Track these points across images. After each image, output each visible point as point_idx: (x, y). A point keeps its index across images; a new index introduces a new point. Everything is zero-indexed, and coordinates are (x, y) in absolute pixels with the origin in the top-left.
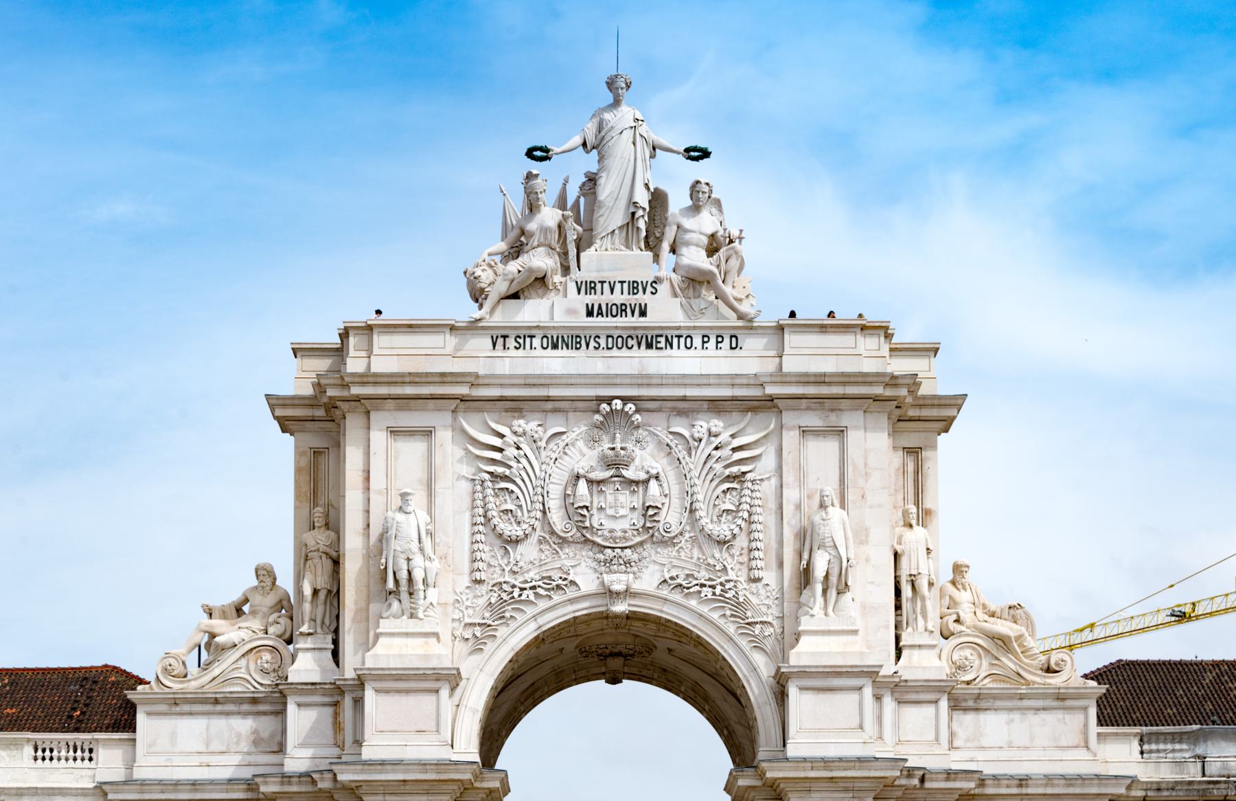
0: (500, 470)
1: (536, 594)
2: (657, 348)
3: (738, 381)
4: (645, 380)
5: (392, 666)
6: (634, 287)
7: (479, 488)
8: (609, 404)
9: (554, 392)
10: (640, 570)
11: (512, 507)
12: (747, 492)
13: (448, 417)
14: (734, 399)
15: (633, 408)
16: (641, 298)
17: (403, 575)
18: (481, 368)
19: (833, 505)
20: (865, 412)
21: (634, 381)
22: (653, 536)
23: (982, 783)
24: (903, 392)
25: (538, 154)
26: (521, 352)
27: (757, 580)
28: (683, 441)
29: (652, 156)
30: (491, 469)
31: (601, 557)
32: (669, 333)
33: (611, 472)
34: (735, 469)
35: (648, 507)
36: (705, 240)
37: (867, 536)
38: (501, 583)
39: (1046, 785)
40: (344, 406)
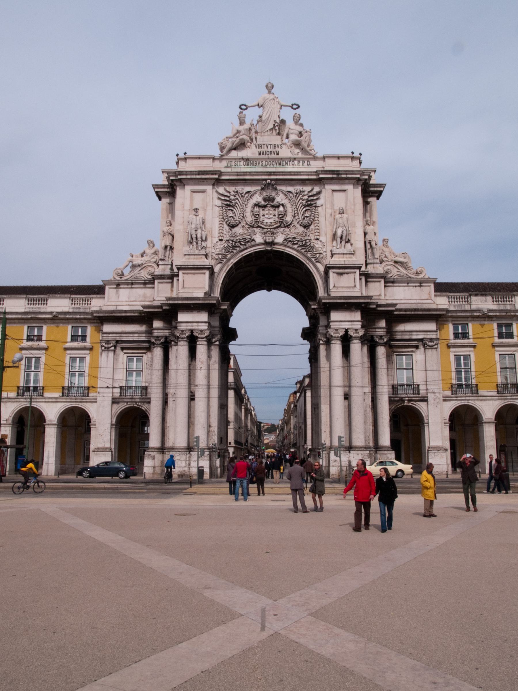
0: (228, 203)
2: (282, 165)
5: (189, 264)
6: (275, 146)
7: (221, 209)
8: (266, 182)
11: (233, 215)
12: (313, 210)
13: (211, 187)
15: (274, 182)
16: (277, 149)
17: (194, 236)
18: (223, 170)
19: (343, 213)
20: (353, 185)
22: (281, 225)
23: (397, 310)
24: (366, 177)
25: (243, 107)
26: (236, 167)
27: (318, 239)
28: (291, 195)
29: (281, 109)
30: (226, 203)
31: (263, 231)
33: (266, 203)
34: (309, 203)
35: (280, 214)
36: (298, 133)
37: (355, 225)
38: (228, 240)
40: (177, 183)
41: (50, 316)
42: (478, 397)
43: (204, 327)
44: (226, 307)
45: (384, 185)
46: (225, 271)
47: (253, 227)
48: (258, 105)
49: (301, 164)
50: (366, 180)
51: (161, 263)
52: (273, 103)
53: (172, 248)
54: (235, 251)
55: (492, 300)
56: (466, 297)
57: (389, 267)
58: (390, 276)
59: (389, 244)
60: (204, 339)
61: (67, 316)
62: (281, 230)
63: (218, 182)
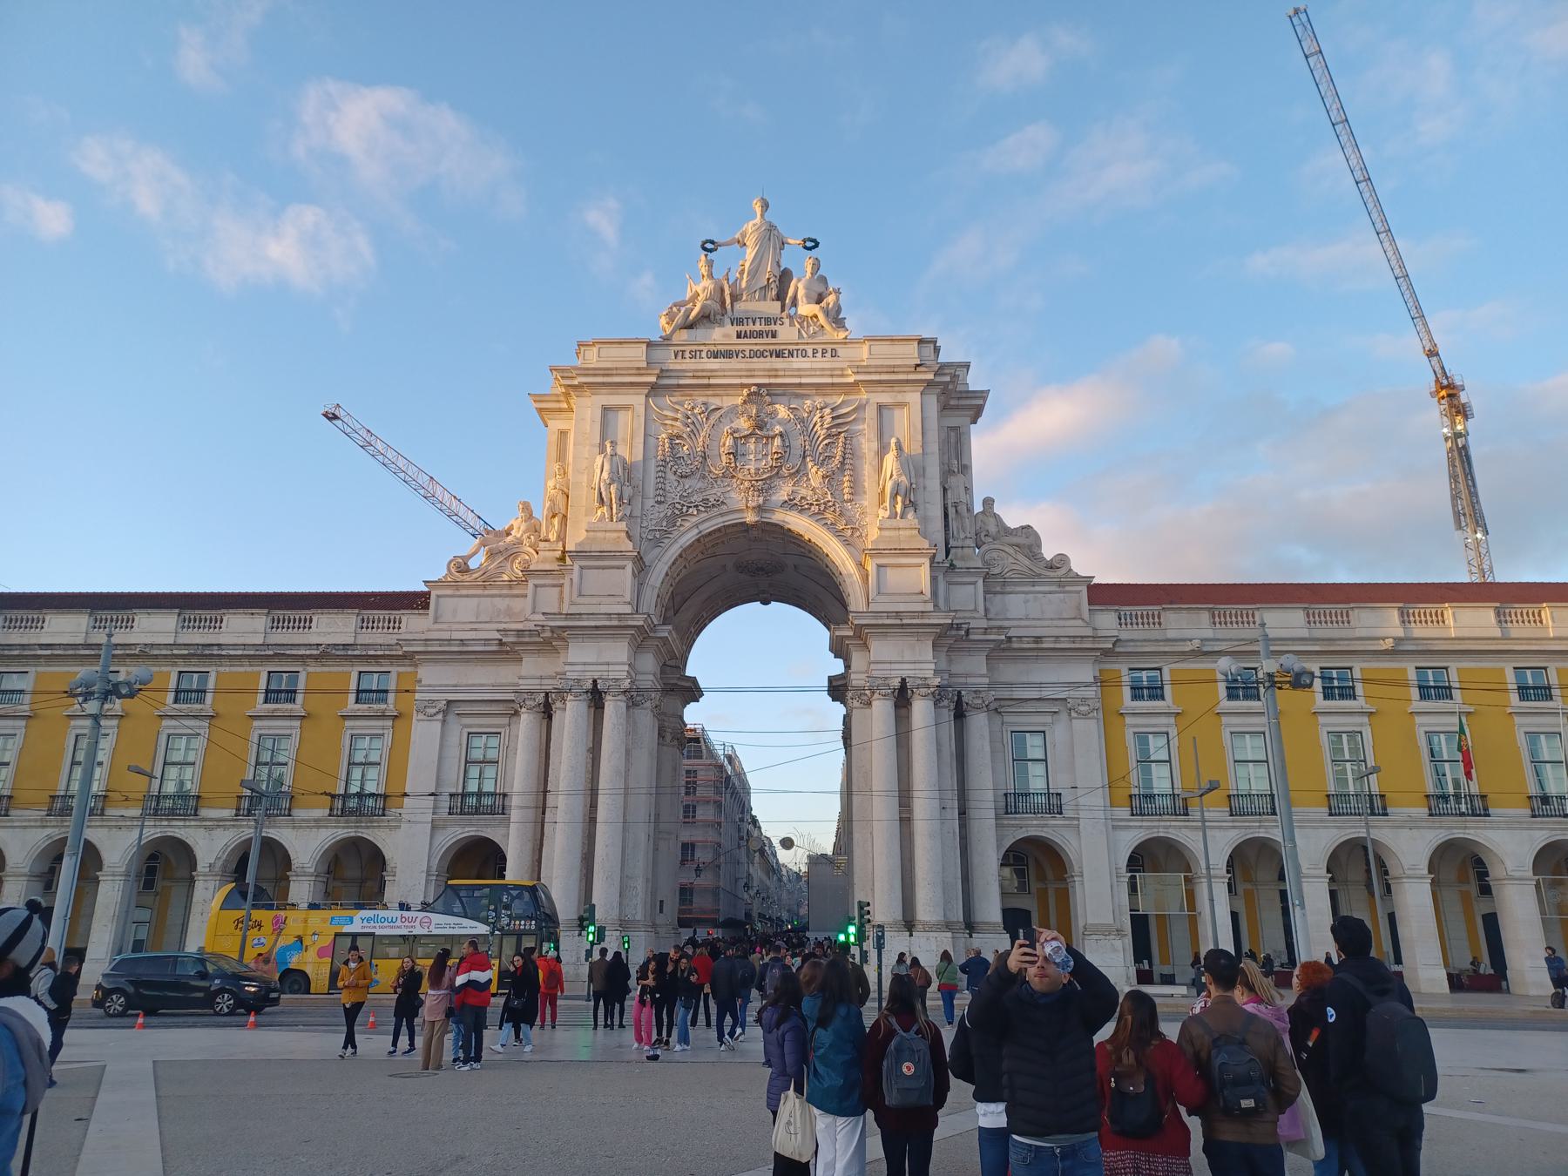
1: (698, 510)
3: (836, 373)
4: (774, 373)
6: (768, 321)
9: (712, 381)
10: (770, 496)
14: (833, 384)
16: (773, 327)
21: (766, 373)
22: (777, 473)
23: (1009, 639)
24: (947, 379)
25: (709, 247)
26: (693, 360)
32: (791, 347)
39: (1055, 642)
41: (315, 652)
42: (1188, 821)
43: (621, 672)
44: (666, 634)
45: (984, 395)
46: (666, 564)
47: (724, 477)
48: (739, 242)
49: (819, 354)
50: (948, 383)
51: (542, 545)
52: (767, 237)
53: (565, 517)
54: (687, 525)
55: (1212, 620)
56: (1156, 613)
57: (995, 555)
58: (996, 571)
59: (997, 509)
60: (619, 698)
61: (350, 653)
62: (779, 482)
63: (654, 389)
